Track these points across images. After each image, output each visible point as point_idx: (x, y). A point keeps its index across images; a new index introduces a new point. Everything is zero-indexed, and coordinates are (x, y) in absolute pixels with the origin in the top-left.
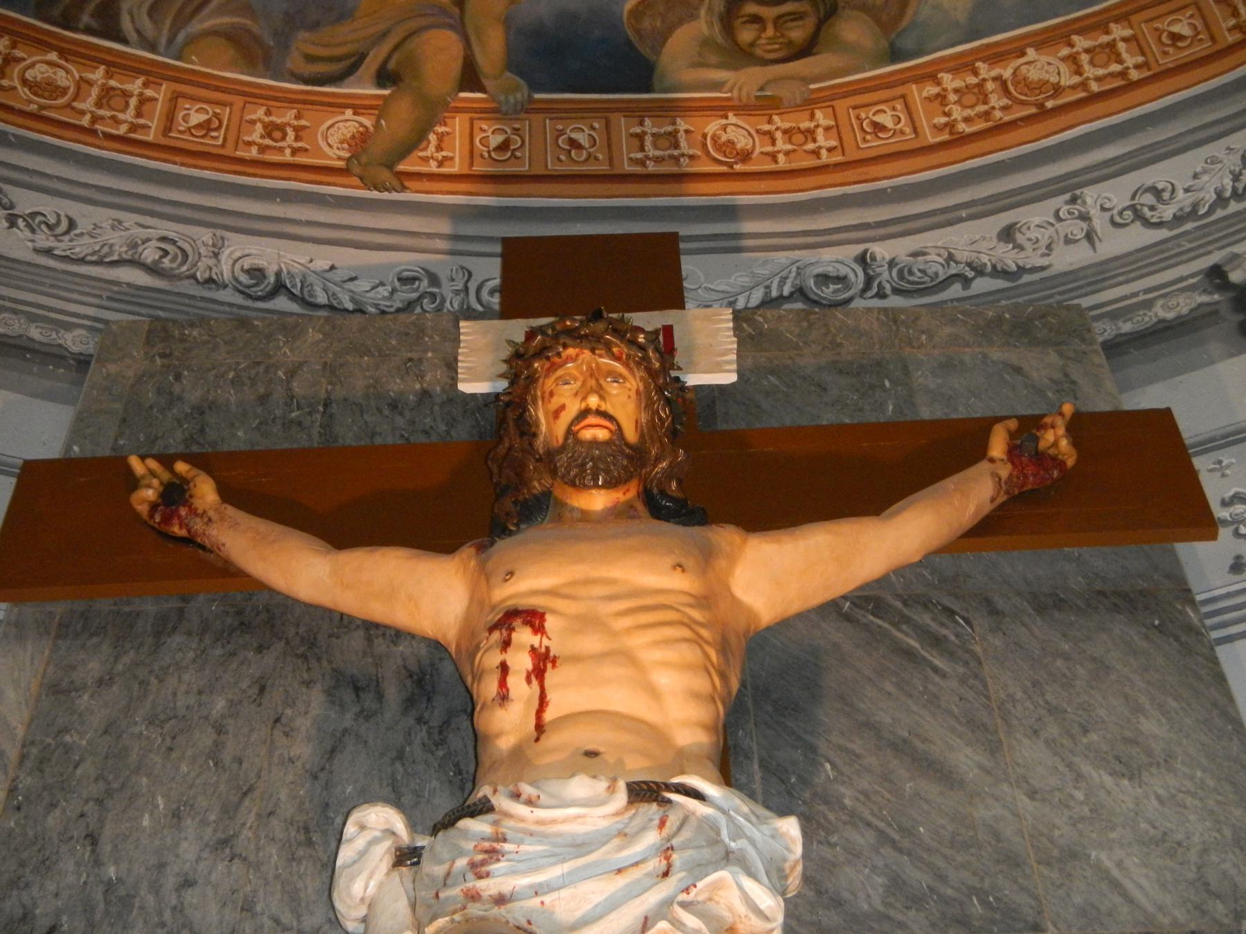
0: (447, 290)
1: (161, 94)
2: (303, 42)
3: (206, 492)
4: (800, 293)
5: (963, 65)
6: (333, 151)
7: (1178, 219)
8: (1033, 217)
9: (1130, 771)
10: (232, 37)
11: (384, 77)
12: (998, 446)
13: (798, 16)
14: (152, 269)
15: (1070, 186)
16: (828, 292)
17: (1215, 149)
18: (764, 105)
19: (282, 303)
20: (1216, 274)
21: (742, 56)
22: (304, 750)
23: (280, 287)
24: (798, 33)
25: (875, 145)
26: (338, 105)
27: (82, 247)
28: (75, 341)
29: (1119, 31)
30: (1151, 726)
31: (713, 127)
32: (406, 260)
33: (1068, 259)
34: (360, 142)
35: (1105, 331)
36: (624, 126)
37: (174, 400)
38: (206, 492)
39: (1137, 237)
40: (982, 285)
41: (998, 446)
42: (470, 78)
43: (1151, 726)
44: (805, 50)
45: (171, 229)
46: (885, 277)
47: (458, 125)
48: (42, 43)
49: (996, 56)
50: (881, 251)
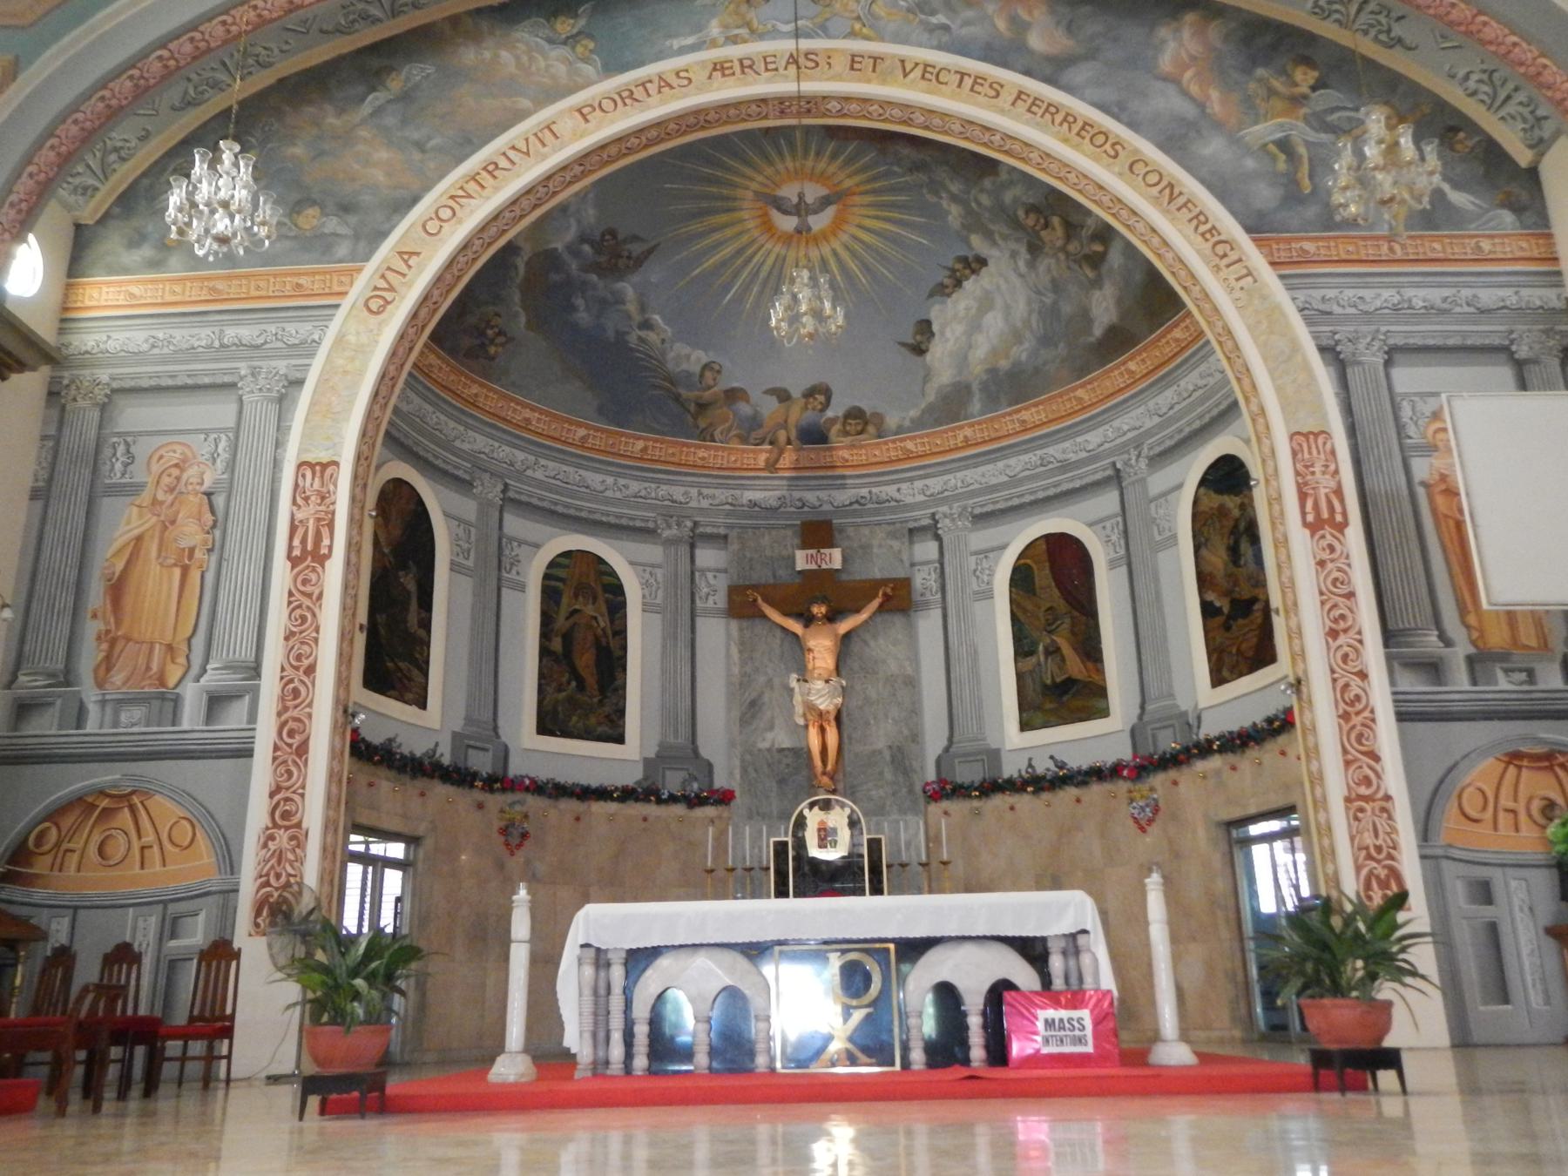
0: (788, 501)
1: (725, 454)
2: (753, 435)
3: (760, 600)
4: (857, 502)
5: (894, 441)
6: (762, 464)
7: (932, 495)
8: (904, 486)
9: (894, 645)
10: (738, 436)
11: (771, 443)
12: (880, 593)
13: (859, 424)
14: (731, 504)
15: (911, 480)
16: (863, 501)
17: (939, 478)
18: (852, 446)
19: (757, 509)
20: (933, 515)
21: (846, 434)
22: (778, 641)
23: (755, 505)
24: (859, 428)
25: (874, 460)
26: (762, 451)
27: (716, 502)
28: (722, 531)
29: (926, 440)
30: (900, 637)
31: (840, 453)
32: (778, 493)
33: (909, 500)
34: (767, 460)
35: (912, 525)
36: (823, 454)
37: (745, 557)
38: (760, 600)
39: (922, 498)
40: (893, 503)
41: (880, 593)
42: (789, 442)
43: (900, 637)
44: (861, 433)
45: (732, 492)
46: (874, 498)
47: (786, 455)
48: (700, 447)
49: (902, 440)
50: (874, 490)
